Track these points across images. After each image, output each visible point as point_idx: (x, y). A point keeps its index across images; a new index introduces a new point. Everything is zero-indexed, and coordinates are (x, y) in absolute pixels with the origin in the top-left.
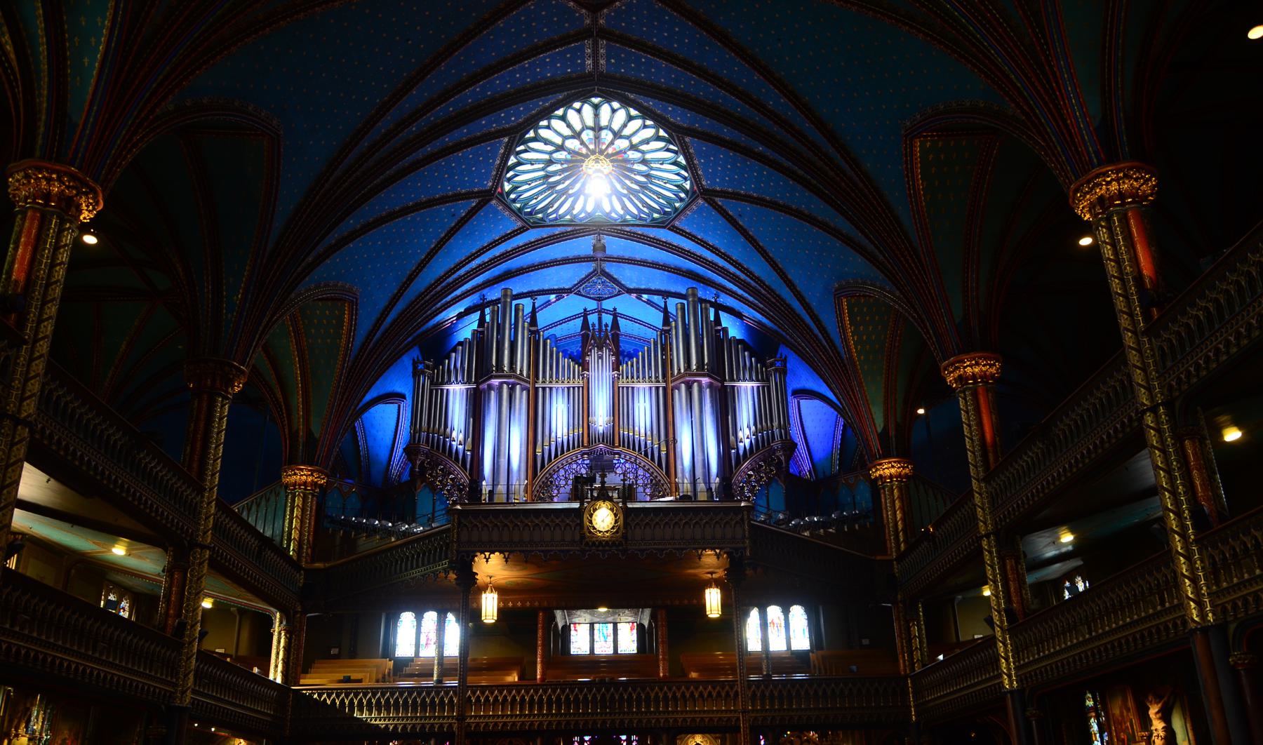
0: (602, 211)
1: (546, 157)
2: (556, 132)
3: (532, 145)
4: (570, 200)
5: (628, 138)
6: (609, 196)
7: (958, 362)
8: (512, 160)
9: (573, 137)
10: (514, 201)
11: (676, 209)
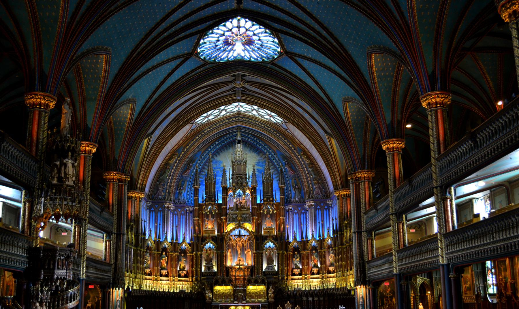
0: (241, 56)
1: (217, 39)
2: (221, 30)
3: (211, 35)
4: (227, 53)
5: (253, 31)
6: (244, 51)
7: (387, 142)
8: (202, 41)
9: (228, 31)
10: (202, 55)
11: (274, 57)
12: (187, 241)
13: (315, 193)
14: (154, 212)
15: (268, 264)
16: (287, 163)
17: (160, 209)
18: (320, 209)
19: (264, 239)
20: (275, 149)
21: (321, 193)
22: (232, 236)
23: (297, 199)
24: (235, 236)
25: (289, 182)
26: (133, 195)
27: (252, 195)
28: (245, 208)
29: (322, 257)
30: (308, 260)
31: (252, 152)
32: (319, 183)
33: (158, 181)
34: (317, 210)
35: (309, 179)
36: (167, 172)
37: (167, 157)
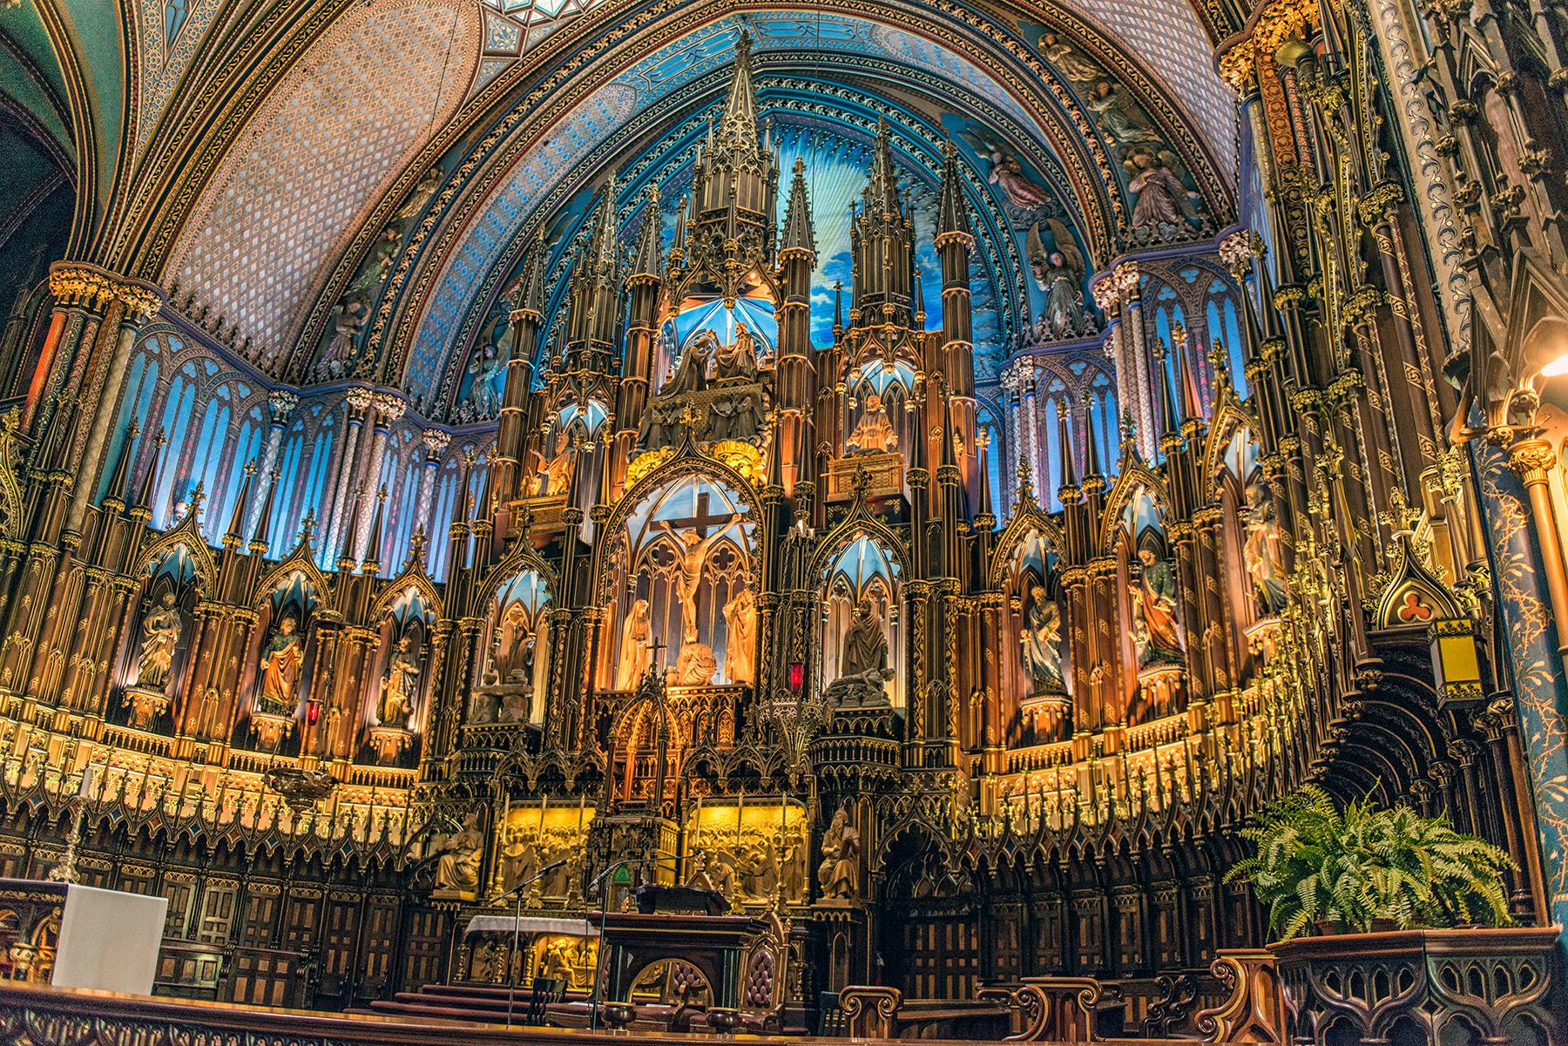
12: (430, 572)
13: (1135, 218)
14: (301, 439)
15: (850, 667)
16: (996, 157)
17: (329, 421)
18: (1180, 301)
19: (830, 516)
20: (934, 111)
21: (1178, 211)
22: (655, 526)
23: (1059, 319)
24: (673, 524)
25: (1016, 247)
26: (78, 287)
27: (779, 305)
28: (740, 373)
29: (1199, 570)
30: (1111, 622)
31: (834, 166)
32: (1159, 165)
33: (343, 302)
34: (1161, 310)
35: (1098, 159)
36: (381, 254)
37: (393, 192)
